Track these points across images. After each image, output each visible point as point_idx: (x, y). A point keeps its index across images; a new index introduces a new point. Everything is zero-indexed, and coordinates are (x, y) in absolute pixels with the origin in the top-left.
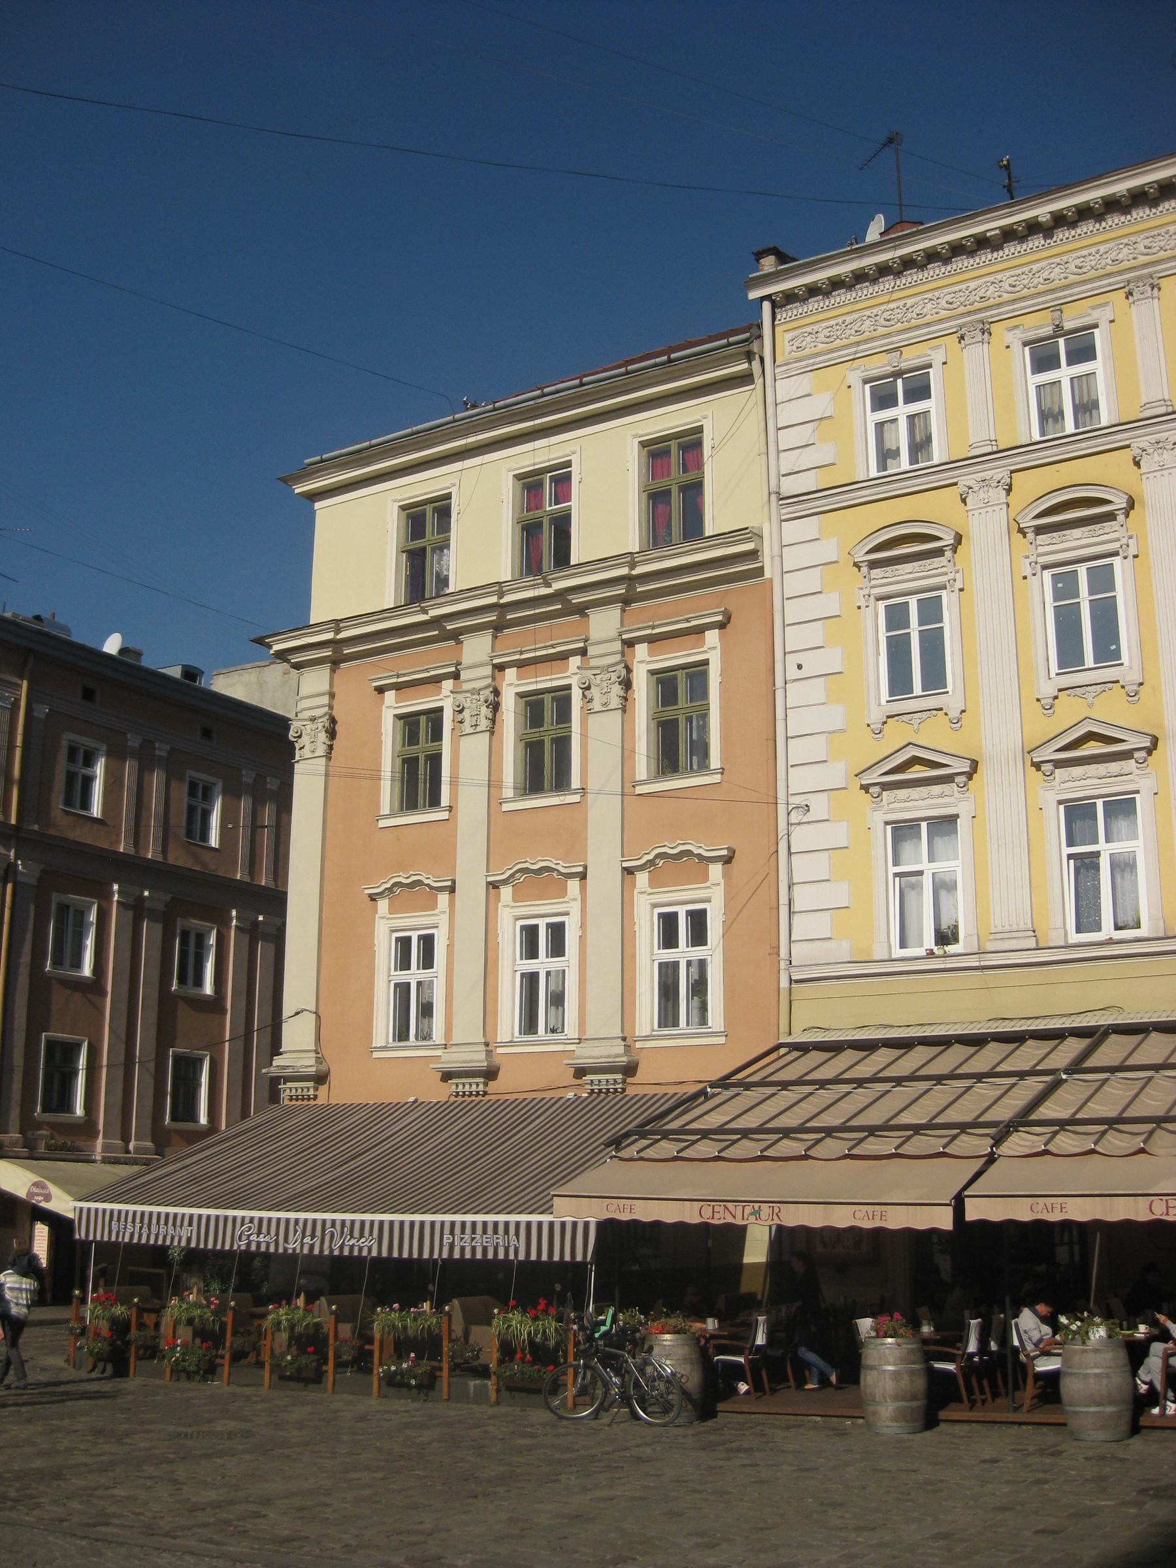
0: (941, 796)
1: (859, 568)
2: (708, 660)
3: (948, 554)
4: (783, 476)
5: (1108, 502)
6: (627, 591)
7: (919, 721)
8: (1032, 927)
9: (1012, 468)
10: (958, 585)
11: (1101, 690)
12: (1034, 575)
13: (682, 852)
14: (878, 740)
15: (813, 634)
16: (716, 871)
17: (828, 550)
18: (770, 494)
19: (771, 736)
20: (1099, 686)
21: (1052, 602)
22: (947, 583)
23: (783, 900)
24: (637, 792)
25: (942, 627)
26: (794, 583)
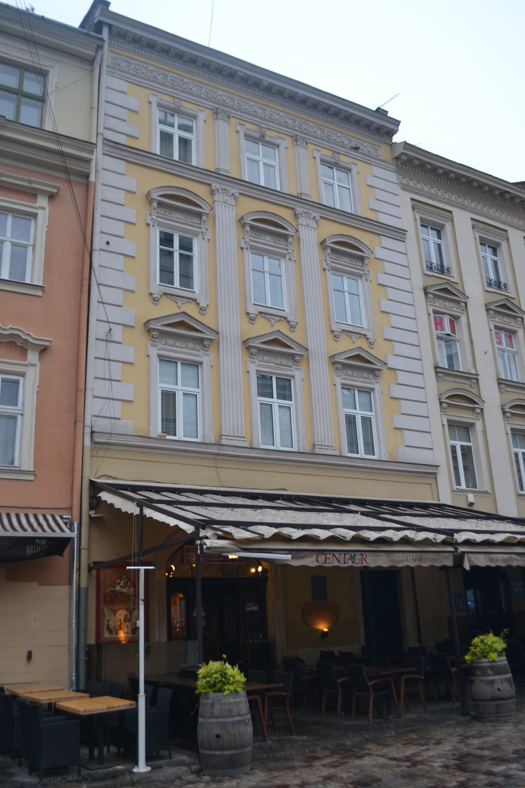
7: (182, 302)
14: (156, 305)
15: (119, 228)
17: (130, 183)
18: (97, 134)
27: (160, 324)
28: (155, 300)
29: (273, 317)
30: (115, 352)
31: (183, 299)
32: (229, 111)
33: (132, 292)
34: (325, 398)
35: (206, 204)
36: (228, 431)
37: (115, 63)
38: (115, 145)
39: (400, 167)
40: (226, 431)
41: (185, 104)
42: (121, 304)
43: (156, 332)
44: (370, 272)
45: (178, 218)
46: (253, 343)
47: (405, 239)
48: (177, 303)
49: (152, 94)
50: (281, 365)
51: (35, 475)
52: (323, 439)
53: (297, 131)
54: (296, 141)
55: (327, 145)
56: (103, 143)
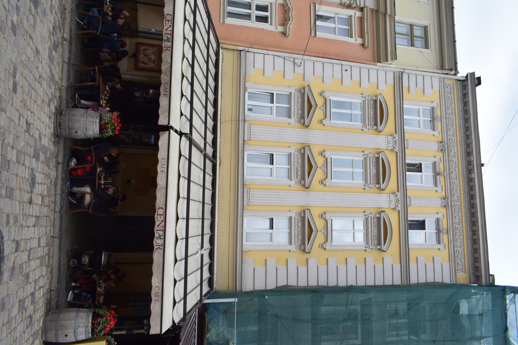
0: (298, 114)
2: (353, 38)
3: (375, 127)
4: (408, 75)
5: (383, 182)
6: (382, 13)
7: (323, 109)
9: (398, 153)
10: (364, 129)
12: (364, 155)
13: (290, 17)
16: (280, 29)
17: (382, 86)
18: (404, 69)
19: (326, 56)
23: (270, 52)
24: (311, 4)
26: (373, 74)
27: (308, 92)
28: (321, 94)
29: (326, 168)
31: (325, 110)
32: (445, 150)
33: (323, 82)
34: (280, 200)
35: (383, 128)
37: (447, 85)
38: (401, 78)
41: (439, 124)
49: (437, 104)
51: (223, 24)
52: (254, 196)
53: (451, 204)
55: (450, 224)
56: (400, 72)
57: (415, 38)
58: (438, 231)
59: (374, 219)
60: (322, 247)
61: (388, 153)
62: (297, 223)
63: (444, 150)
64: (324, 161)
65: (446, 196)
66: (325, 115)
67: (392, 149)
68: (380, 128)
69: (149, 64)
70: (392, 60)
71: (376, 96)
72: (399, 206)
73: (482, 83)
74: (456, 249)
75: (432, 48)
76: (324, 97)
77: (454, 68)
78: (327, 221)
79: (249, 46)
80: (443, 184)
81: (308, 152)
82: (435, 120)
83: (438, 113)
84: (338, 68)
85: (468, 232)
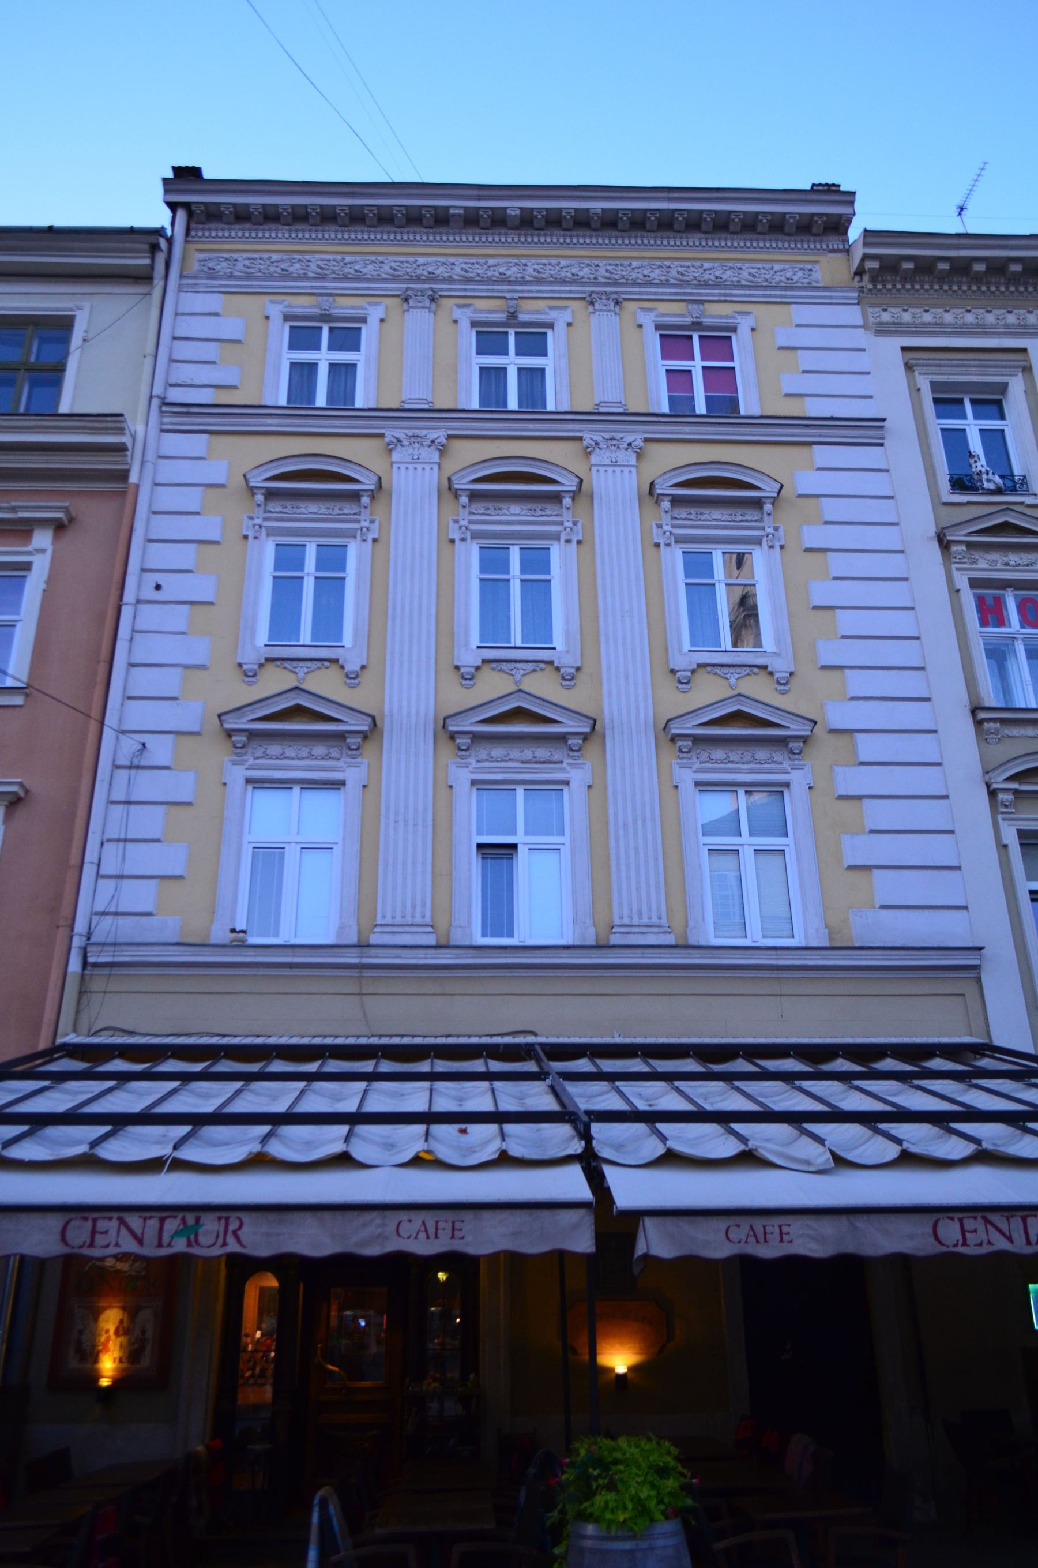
0: (327, 757)
1: (253, 494)
3: (365, 500)
7: (306, 670)
8: (432, 920)
11: (532, 669)
12: (463, 540)
14: (249, 684)
15: (184, 556)
17: (216, 471)
18: (151, 397)
20: (531, 664)
21: (478, 573)
22: (359, 532)
23: (91, 855)
25: (344, 579)
26: (168, 499)
27: (245, 720)
28: (250, 675)
29: (518, 665)
30: (147, 786)
31: (309, 664)
32: (432, 289)
33: (202, 667)
34: (644, 821)
36: (398, 915)
37: (205, 269)
38: (184, 410)
39: (870, 290)
40: (384, 917)
41: (341, 301)
42: (175, 695)
43: (240, 736)
44: (781, 529)
45: (311, 513)
46: (460, 726)
47: (883, 438)
48: (295, 672)
50: (536, 762)
54: (592, 303)
55: (671, 294)
56: (161, 412)
57: (33, 359)
58: (698, 330)
59: (676, 518)
60: (784, 684)
61: (451, 466)
62: (716, 765)
63: (430, 293)
64: (493, 669)
65: (584, 299)
66: (327, 664)
67: (440, 450)
68: (368, 483)
69: (144, 1332)
70: (121, 431)
71: (252, 490)
72: (629, 438)
73: (197, 165)
74: (744, 283)
75: (71, 305)
76: (261, 666)
77: (152, 239)
78: (699, 666)
79: (62, 933)
80: (542, 304)
81: (468, 722)
82: (329, 315)
83: (306, 304)
84: (150, 617)
85: (691, 243)
